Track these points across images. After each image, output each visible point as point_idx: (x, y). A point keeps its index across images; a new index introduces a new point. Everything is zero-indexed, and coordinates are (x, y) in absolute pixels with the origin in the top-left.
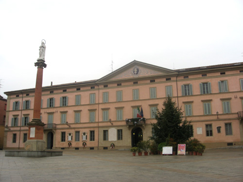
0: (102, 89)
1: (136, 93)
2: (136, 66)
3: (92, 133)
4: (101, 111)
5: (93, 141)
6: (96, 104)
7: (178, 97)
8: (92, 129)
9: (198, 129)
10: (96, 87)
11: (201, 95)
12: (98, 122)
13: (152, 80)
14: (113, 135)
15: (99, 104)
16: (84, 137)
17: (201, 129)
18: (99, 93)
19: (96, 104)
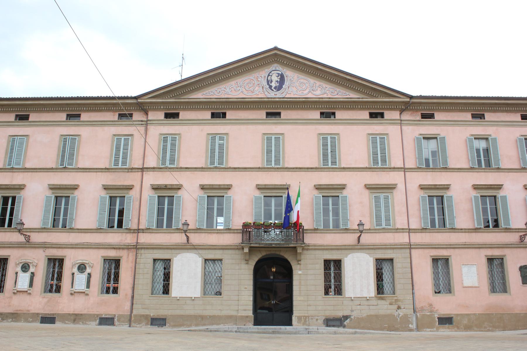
0: (157, 122)
2: (275, 66)
4: (148, 194)
5: (111, 296)
6: (132, 170)
7: (404, 168)
8: (112, 254)
9: (465, 269)
10: (138, 116)
12: (138, 231)
14: (188, 275)
15: (143, 169)
16: (81, 279)
17: (474, 269)
18: (147, 139)
19: (132, 170)
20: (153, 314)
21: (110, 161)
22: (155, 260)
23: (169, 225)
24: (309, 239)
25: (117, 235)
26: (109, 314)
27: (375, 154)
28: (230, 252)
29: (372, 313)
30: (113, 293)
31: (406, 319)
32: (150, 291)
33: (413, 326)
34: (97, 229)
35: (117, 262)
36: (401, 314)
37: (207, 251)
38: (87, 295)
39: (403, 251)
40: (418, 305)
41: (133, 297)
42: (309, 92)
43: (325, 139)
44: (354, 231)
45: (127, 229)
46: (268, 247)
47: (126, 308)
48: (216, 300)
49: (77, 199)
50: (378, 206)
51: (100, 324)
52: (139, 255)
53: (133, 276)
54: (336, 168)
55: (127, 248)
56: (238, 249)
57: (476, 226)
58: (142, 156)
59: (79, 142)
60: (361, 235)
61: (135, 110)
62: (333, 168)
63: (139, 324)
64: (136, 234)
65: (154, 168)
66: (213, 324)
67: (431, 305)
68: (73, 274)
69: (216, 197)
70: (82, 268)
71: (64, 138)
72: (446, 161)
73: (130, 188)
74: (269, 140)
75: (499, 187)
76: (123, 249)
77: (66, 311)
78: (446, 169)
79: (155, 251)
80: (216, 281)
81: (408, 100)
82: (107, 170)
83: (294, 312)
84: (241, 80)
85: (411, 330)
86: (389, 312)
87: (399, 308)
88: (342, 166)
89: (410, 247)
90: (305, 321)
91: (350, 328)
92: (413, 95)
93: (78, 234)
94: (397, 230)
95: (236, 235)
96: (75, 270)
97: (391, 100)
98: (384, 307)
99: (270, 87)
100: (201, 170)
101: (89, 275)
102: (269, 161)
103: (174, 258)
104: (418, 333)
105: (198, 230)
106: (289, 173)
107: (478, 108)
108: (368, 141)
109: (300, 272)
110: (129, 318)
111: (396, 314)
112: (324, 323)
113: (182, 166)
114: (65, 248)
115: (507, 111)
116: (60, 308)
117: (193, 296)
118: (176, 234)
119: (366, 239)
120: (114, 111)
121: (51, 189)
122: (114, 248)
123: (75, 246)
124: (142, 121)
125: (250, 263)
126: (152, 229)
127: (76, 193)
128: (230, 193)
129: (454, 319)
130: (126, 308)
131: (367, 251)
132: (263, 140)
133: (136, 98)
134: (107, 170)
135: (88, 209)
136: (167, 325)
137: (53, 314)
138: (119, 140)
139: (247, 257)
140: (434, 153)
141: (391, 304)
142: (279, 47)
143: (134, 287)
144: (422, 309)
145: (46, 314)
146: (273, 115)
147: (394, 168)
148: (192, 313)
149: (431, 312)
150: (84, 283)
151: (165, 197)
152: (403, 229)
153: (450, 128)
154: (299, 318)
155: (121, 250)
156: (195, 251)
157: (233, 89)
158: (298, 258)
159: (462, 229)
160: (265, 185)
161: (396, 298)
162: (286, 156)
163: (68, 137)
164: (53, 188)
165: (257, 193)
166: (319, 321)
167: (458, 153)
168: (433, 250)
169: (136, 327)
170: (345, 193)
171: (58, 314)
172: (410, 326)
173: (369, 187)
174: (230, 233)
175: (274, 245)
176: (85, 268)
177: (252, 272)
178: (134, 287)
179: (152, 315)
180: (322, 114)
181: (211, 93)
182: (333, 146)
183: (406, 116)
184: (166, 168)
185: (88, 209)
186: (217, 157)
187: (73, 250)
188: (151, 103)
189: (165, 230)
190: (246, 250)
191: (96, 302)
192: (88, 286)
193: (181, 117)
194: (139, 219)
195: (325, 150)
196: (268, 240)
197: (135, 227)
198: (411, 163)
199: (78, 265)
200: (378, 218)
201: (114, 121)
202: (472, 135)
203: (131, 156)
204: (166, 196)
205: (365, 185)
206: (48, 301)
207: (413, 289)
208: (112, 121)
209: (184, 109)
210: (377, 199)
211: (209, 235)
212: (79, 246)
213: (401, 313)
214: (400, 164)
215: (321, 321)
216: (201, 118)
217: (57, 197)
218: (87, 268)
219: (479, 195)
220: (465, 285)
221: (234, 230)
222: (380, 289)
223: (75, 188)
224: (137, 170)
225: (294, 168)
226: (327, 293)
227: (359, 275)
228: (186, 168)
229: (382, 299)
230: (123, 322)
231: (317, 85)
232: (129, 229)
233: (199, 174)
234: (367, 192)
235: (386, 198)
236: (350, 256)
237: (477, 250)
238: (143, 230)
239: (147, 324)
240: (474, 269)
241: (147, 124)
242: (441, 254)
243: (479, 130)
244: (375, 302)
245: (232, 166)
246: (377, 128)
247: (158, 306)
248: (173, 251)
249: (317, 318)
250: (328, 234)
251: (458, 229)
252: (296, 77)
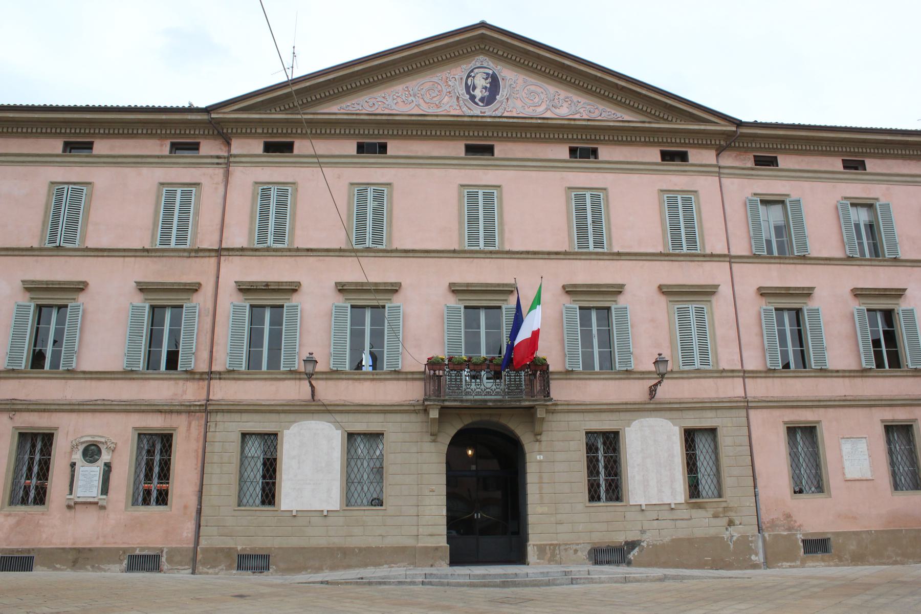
0: (250, 160)
1: (480, 209)
2: (481, 60)
3: (156, 452)
4: (229, 299)
5: (154, 510)
6: (198, 252)
8: (156, 423)
9: (846, 447)
10: (208, 147)
11: (849, 260)
12: (210, 375)
13: (584, 146)
15: (220, 252)
16: (89, 476)
17: (863, 446)
18: (227, 195)
19: (198, 252)
20: (241, 545)
21: (153, 236)
22: (244, 435)
23: (274, 362)
24: (560, 391)
25: (166, 383)
26: (149, 548)
27: (675, 228)
28: (398, 417)
29: (681, 534)
30: (158, 503)
31: (744, 544)
32: (234, 500)
33: (759, 558)
34: (125, 372)
35: (166, 440)
36: (736, 535)
37: (351, 417)
38: (103, 508)
39: (734, 413)
40: (765, 517)
41: (199, 512)
42: (547, 109)
43: (580, 199)
44: (643, 375)
45: (186, 371)
46: (479, 407)
47: (185, 534)
48: (371, 515)
49: (84, 311)
50: (684, 327)
51: (131, 568)
52: (212, 425)
53: (199, 469)
54: (603, 254)
55: (188, 410)
56: (415, 412)
57: (864, 365)
58: (219, 227)
59: (90, 196)
60: (660, 382)
61: (205, 136)
62: (597, 254)
63: (213, 567)
64: (206, 382)
65: (242, 249)
66: (366, 565)
67: (788, 516)
68: (73, 465)
69: (368, 305)
70: (91, 452)
71: (57, 188)
72: (805, 244)
73: (193, 289)
74: (472, 197)
75: (898, 294)
76: (179, 412)
77: (57, 542)
78: (804, 259)
79: (245, 417)
80: (372, 477)
81: (734, 129)
82: (145, 252)
83: (530, 537)
84: (414, 83)
85: (755, 566)
86: (712, 532)
87: (731, 523)
88: (615, 250)
89: (747, 405)
90: (553, 555)
91: (640, 565)
92: (745, 119)
93: (83, 382)
94: (723, 374)
95: (410, 383)
96: (78, 457)
97: (703, 127)
98: (702, 523)
99: (473, 98)
100: (337, 254)
101: (108, 467)
102: (473, 238)
103: (285, 432)
104: (769, 571)
105: (333, 374)
106: (514, 262)
107: (855, 149)
108: (661, 203)
109: (540, 457)
110: (191, 555)
111: (726, 535)
112: (590, 558)
113: (300, 246)
114: (56, 411)
115: (904, 157)
116: (44, 536)
117: (325, 507)
118: (287, 382)
119: (668, 390)
120: (162, 137)
121: (28, 290)
122: (160, 411)
123: (76, 407)
124: (218, 157)
125: (439, 439)
126: (239, 372)
127: (82, 298)
128: (397, 300)
129: (833, 542)
130: (185, 534)
131: (668, 414)
132: (460, 196)
133: (208, 110)
134: (145, 252)
135: (106, 331)
136: (273, 568)
137: (29, 551)
138: (171, 195)
139: (435, 429)
140: (779, 230)
141: (716, 516)
142: (489, 22)
143: (201, 492)
144: (773, 524)
145: (12, 551)
146: (480, 150)
147: (712, 255)
148: (322, 542)
149: (789, 529)
150: (96, 483)
151: (264, 306)
152: (733, 371)
153: (806, 185)
154: (541, 549)
155: (174, 416)
156: (328, 416)
157: (399, 100)
158: (537, 429)
159: (837, 371)
160: (468, 285)
161: (724, 505)
162: (506, 228)
163: (66, 186)
164: (32, 288)
165: (452, 301)
166: (579, 553)
167: (822, 232)
168: (788, 411)
169: (207, 573)
170: (622, 301)
171: (39, 551)
172: (753, 557)
173: (666, 291)
174: (398, 379)
175: (490, 404)
176: (99, 452)
177: (443, 459)
178: (201, 492)
179: (239, 548)
180: (573, 151)
181: (357, 107)
182: (596, 211)
183: (728, 160)
184: (268, 249)
185: (106, 331)
186: (369, 230)
187: (74, 416)
188: (237, 121)
189: (264, 373)
190: (434, 414)
191: (121, 523)
192: (105, 490)
193: (296, 151)
194: (211, 352)
195: (581, 218)
196: (478, 394)
197: (203, 367)
198: (740, 247)
199: (84, 445)
200: (687, 349)
201: (162, 157)
202: (846, 198)
203: (196, 224)
204: (268, 303)
205: (660, 288)
206: (18, 523)
207: (755, 487)
208: (158, 157)
209: (303, 136)
210: (683, 314)
211: (357, 384)
212: (85, 407)
213: (735, 532)
214: (720, 248)
215: (583, 554)
216: (337, 153)
217: (40, 308)
218: (104, 451)
219: (864, 308)
220: (849, 476)
221: (406, 373)
222: (694, 489)
223: (80, 288)
224: (207, 254)
225: (522, 253)
226: (594, 496)
227: (653, 460)
228: (308, 250)
229: (699, 506)
230: (180, 563)
231: (562, 97)
232: (192, 373)
233: (335, 261)
234: (663, 300)
235: (700, 312)
236: (636, 424)
237: (867, 410)
238: (220, 373)
239: (229, 567)
240: (863, 446)
241: (228, 164)
242: (803, 419)
243: (857, 189)
244: (685, 513)
245: (400, 247)
246: (676, 179)
247: (252, 529)
248: (282, 415)
249: (575, 547)
250: (592, 382)
251: (832, 371)
252: (520, 81)
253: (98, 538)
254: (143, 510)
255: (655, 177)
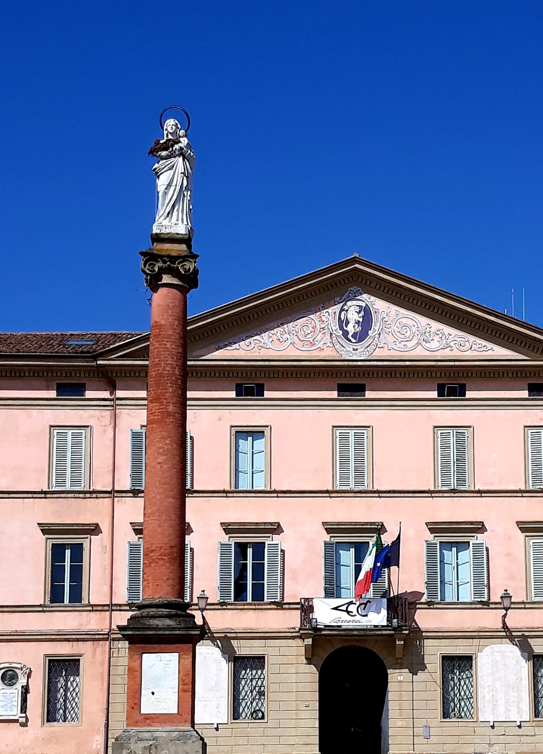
8: (63, 649)
15: (113, 493)
42: (418, 344)
64: (108, 613)
99: (345, 334)
102: (344, 478)
122: (68, 640)
130: (94, 746)
192: (24, 709)
234: (521, 536)
253: (19, 750)
254: (56, 727)
255: (521, 412)
